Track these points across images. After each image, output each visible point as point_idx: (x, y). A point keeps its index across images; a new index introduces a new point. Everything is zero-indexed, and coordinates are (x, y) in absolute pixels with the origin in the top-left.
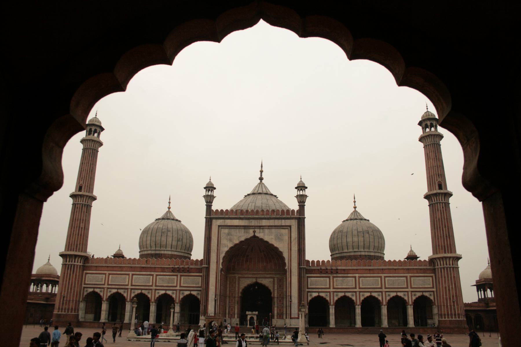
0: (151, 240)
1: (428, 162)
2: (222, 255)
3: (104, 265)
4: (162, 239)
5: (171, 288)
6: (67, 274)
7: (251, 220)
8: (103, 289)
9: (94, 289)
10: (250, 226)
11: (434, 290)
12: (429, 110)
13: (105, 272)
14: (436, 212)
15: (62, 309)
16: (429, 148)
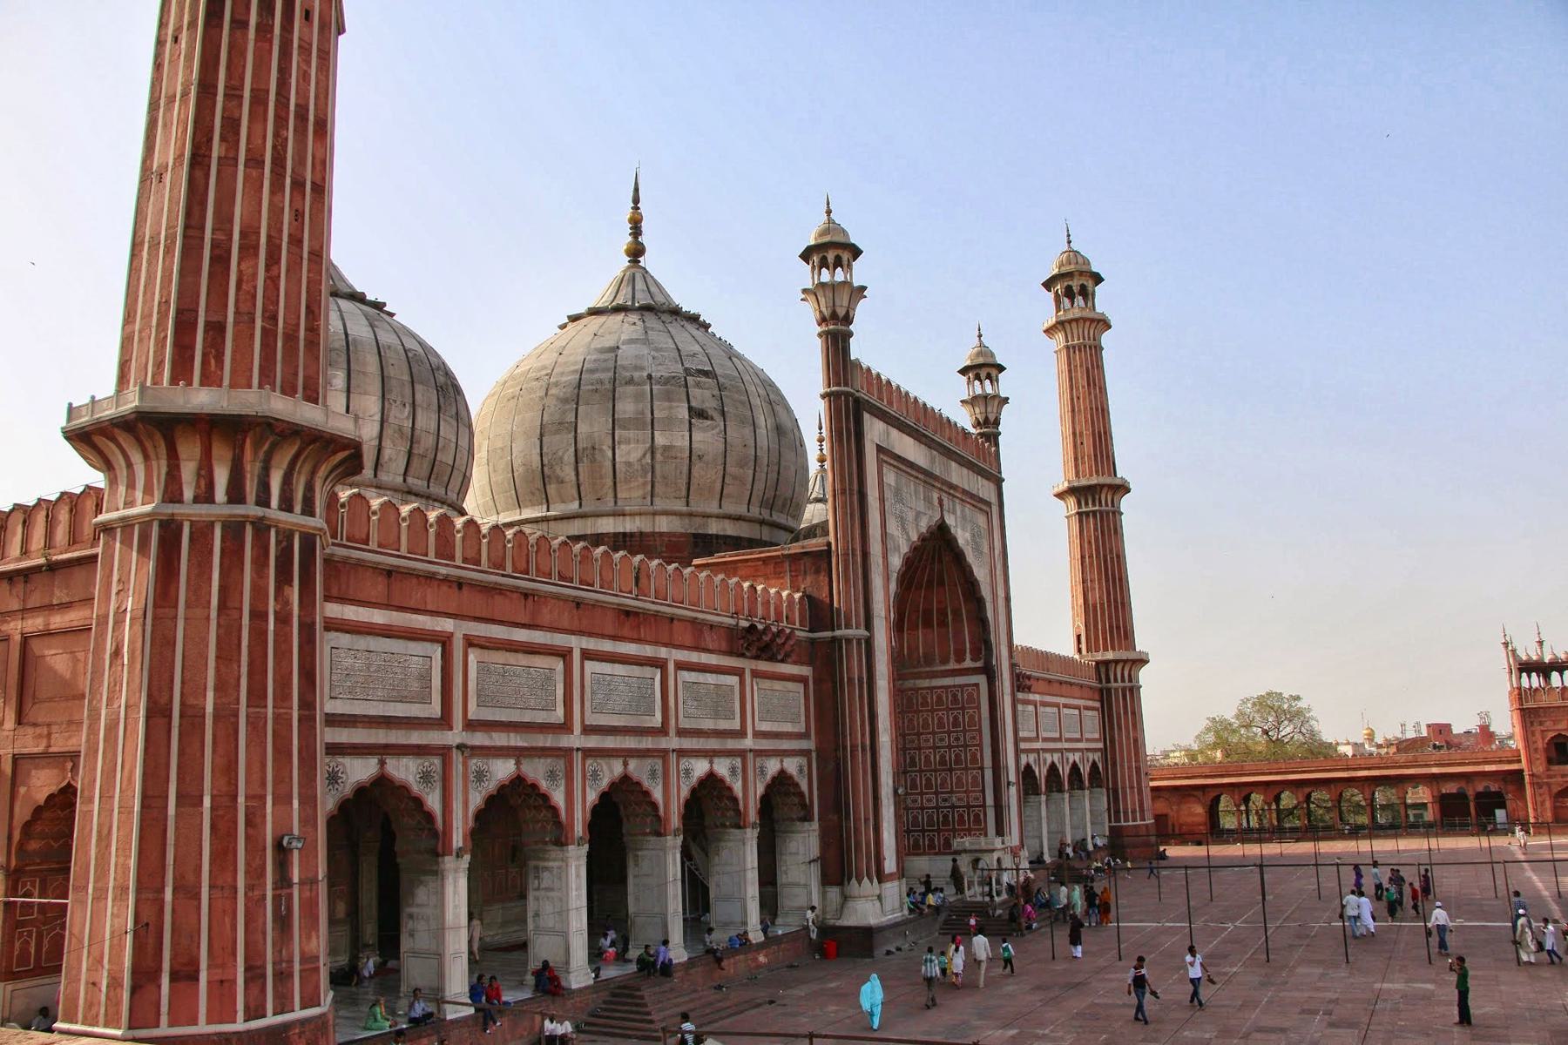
0: (382, 422)
1: (1090, 394)
2: (893, 586)
3: (443, 570)
4: (441, 433)
5: (731, 744)
6: (283, 619)
7: (935, 453)
8: (437, 761)
9: (382, 763)
10: (936, 478)
11: (1100, 745)
12: (1074, 246)
13: (447, 625)
14: (1110, 535)
15: (283, 976)
16: (1091, 355)
